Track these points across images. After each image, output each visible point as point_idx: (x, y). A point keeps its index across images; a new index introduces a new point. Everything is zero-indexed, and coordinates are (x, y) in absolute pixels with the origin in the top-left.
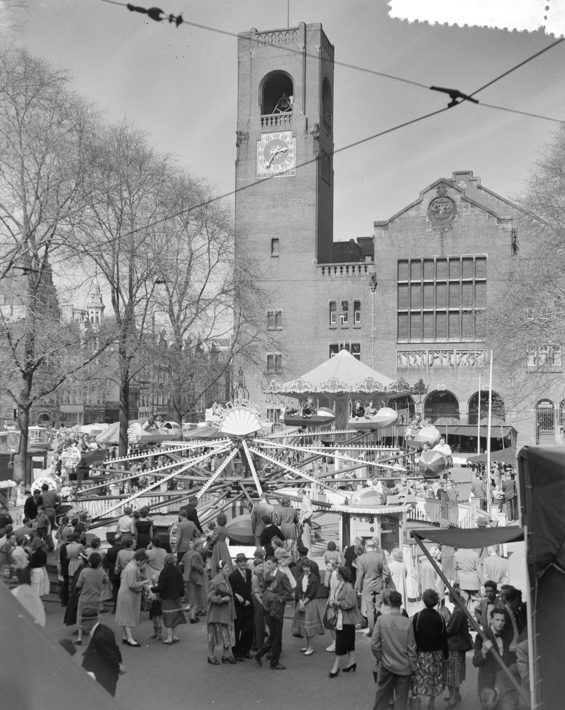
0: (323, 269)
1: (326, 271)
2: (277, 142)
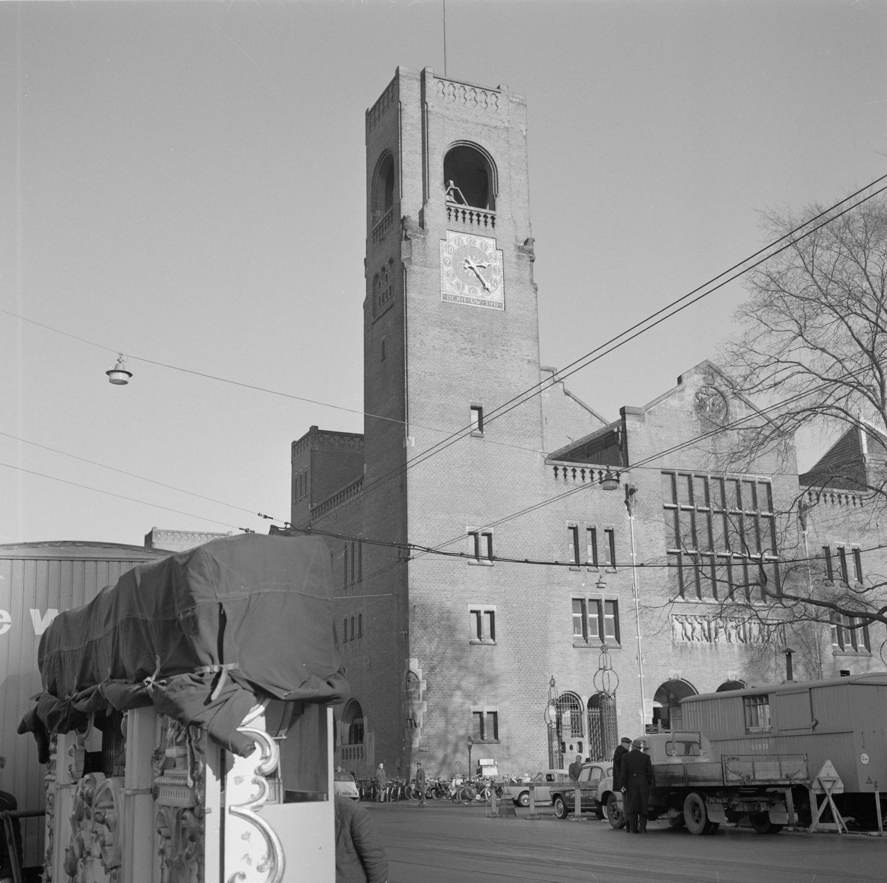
0: (556, 469)
1: (561, 473)
2: (472, 250)
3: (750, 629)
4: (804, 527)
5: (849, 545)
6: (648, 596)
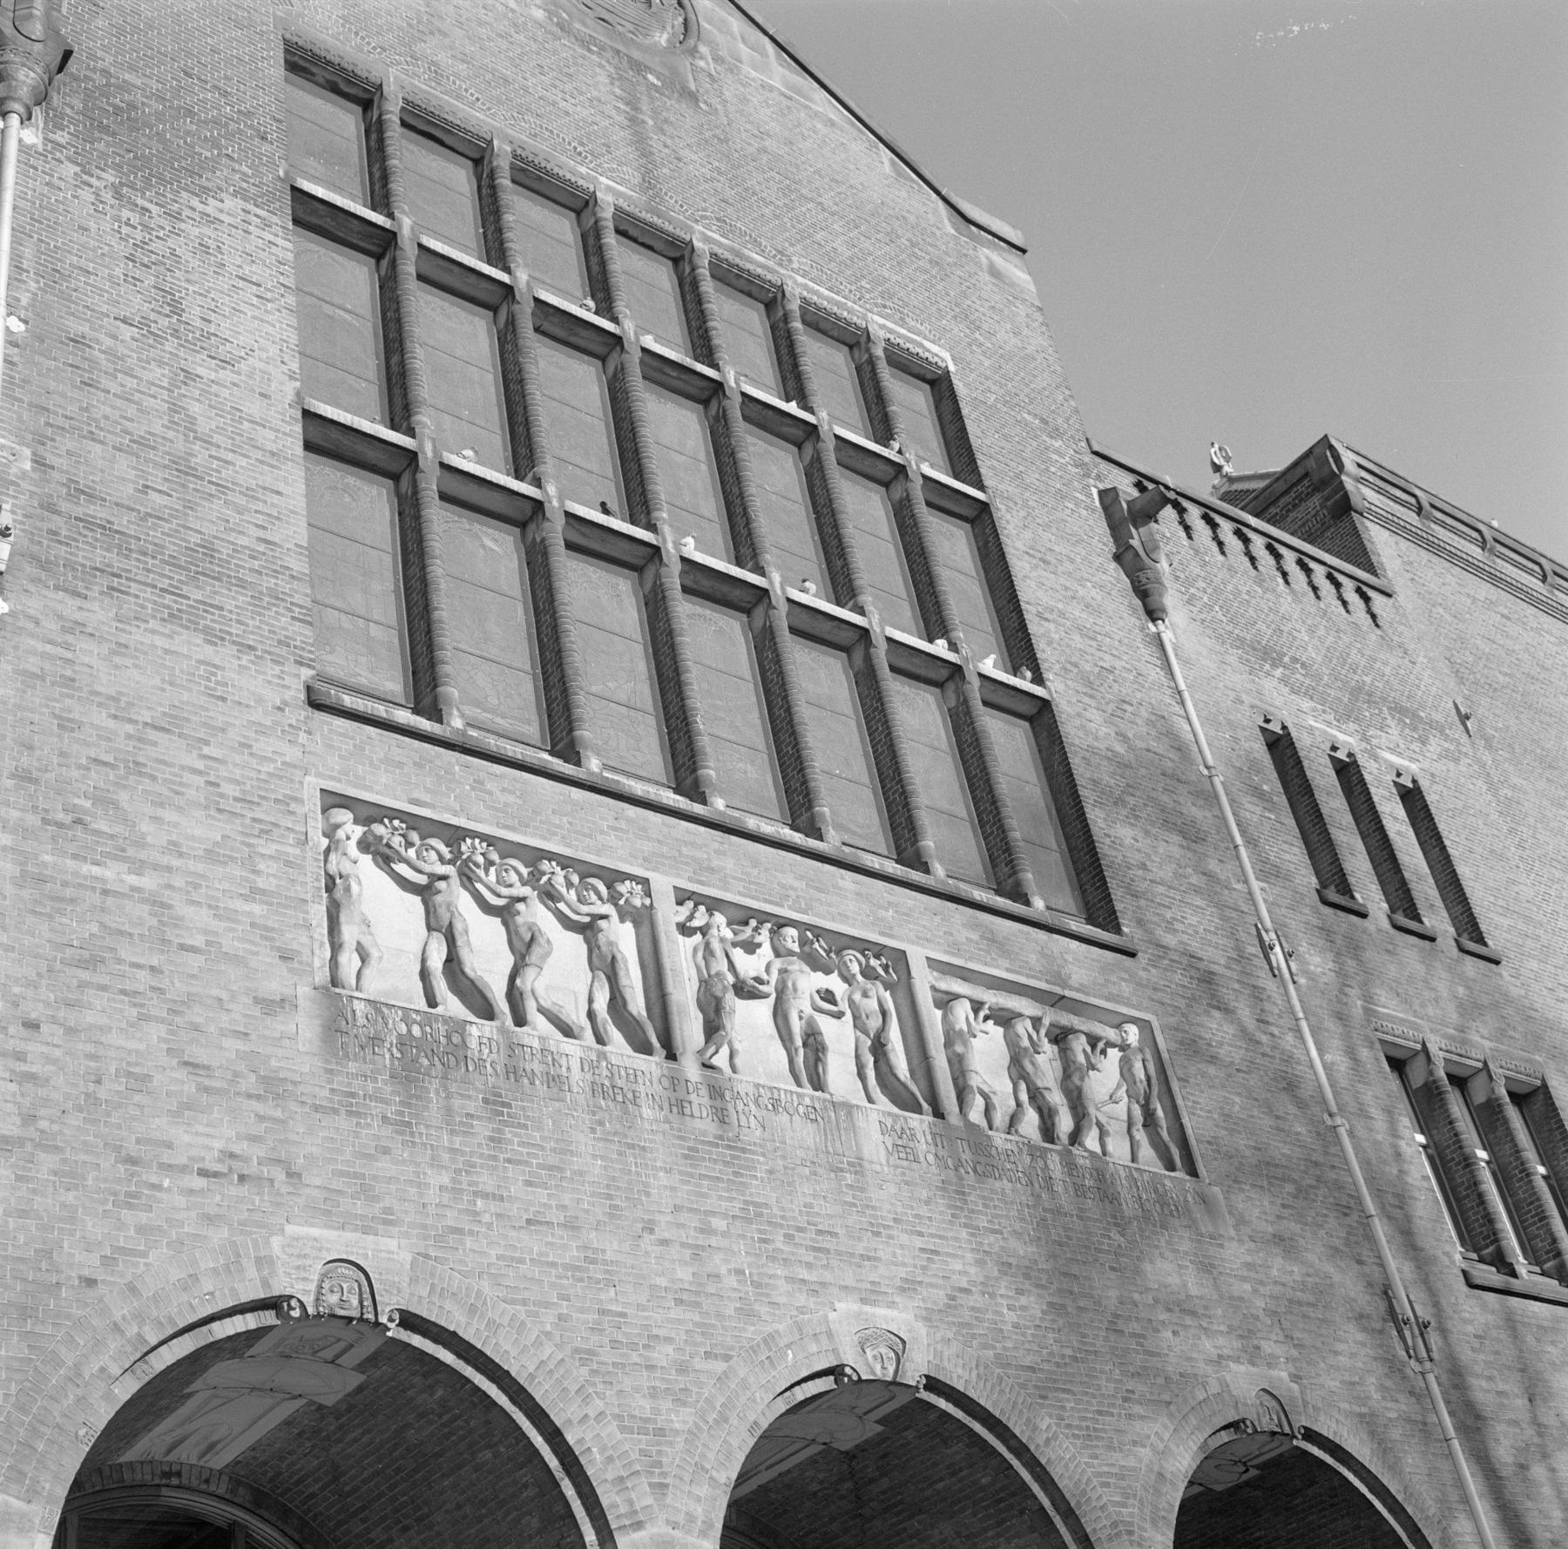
3: (951, 1037)
4: (1153, 613)
5: (1376, 758)
6: (99, 613)
